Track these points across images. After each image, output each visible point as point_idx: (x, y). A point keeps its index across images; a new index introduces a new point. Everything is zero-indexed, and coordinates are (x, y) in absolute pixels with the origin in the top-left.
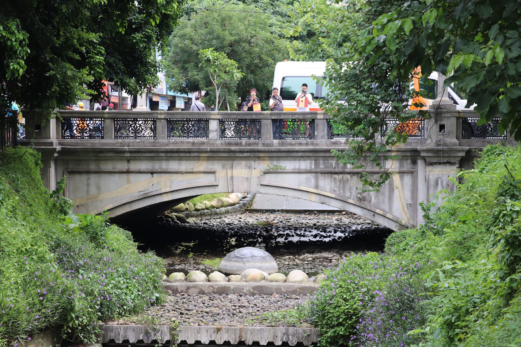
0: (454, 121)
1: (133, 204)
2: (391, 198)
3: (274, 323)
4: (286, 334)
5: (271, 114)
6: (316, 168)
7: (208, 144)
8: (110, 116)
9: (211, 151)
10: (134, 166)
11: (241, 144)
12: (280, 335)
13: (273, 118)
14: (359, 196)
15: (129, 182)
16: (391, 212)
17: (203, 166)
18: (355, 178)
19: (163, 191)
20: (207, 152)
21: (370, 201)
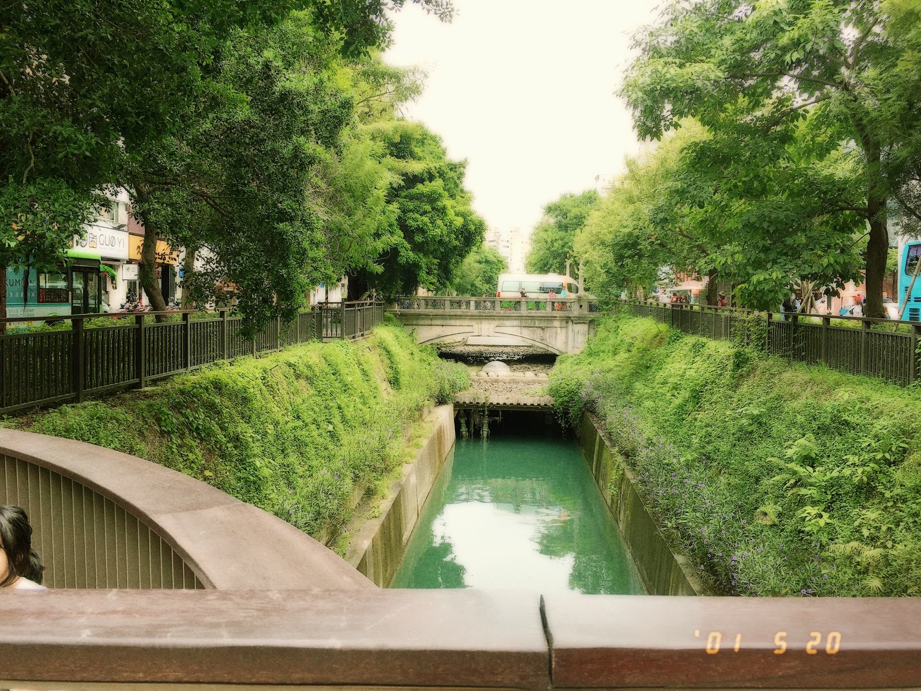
0: (587, 303)
2: (556, 338)
4: (540, 400)
10: (434, 322)
17: (466, 322)
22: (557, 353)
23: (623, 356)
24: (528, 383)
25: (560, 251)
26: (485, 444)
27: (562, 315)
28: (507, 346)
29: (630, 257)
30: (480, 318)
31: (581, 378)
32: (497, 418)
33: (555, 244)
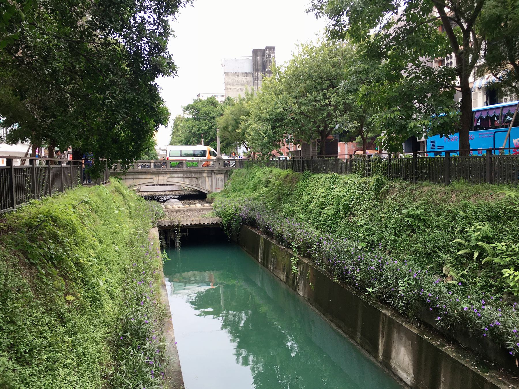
3: (208, 217)
4: (213, 220)
7: (151, 170)
10: (127, 177)
11: (161, 170)
12: (211, 221)
15: (126, 182)
16: (205, 188)
17: (149, 176)
22: (207, 192)
23: (263, 190)
24: (199, 210)
25: (197, 133)
26: (179, 250)
27: (208, 169)
28: (166, 191)
29: (280, 126)
30: (158, 173)
31: (238, 205)
32: (185, 234)
33: (194, 128)
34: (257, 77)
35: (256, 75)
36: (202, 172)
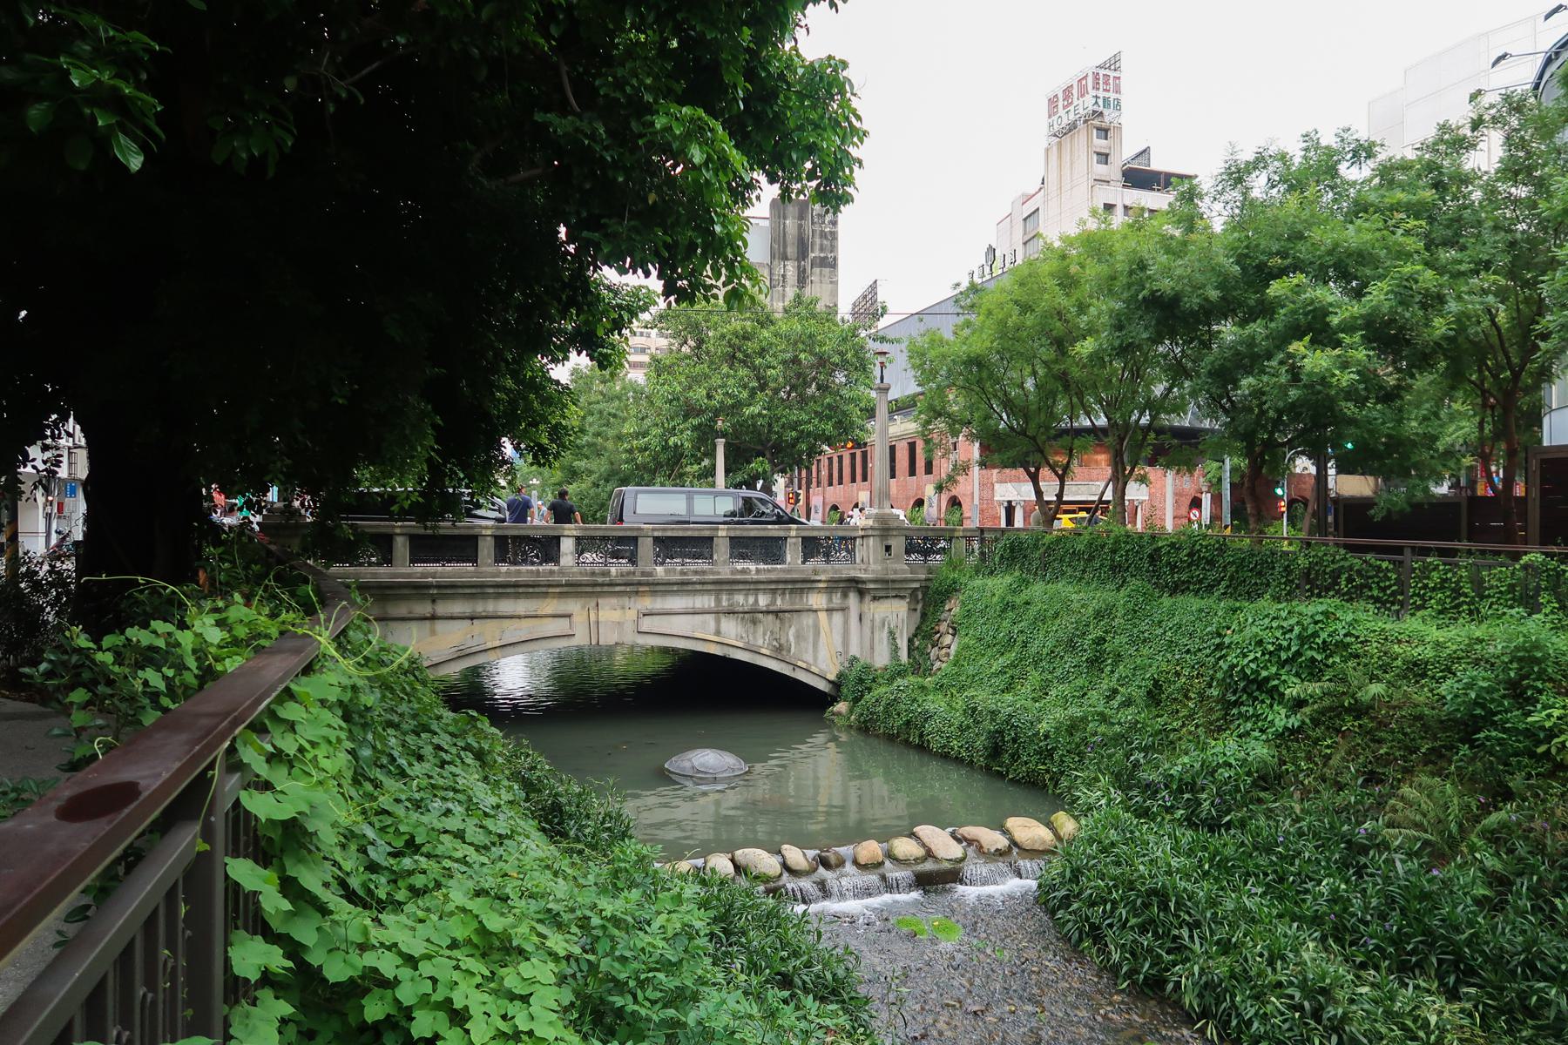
1: (440, 667)
5: (653, 530)
6: (717, 606)
7: (561, 573)
8: (405, 531)
9: (567, 585)
10: (443, 608)
13: (656, 534)
14: (775, 643)
17: (550, 606)
18: (770, 617)
19: (489, 645)
20: (562, 586)
21: (789, 651)
34: (784, 276)
35: (779, 270)
36: (801, 586)
